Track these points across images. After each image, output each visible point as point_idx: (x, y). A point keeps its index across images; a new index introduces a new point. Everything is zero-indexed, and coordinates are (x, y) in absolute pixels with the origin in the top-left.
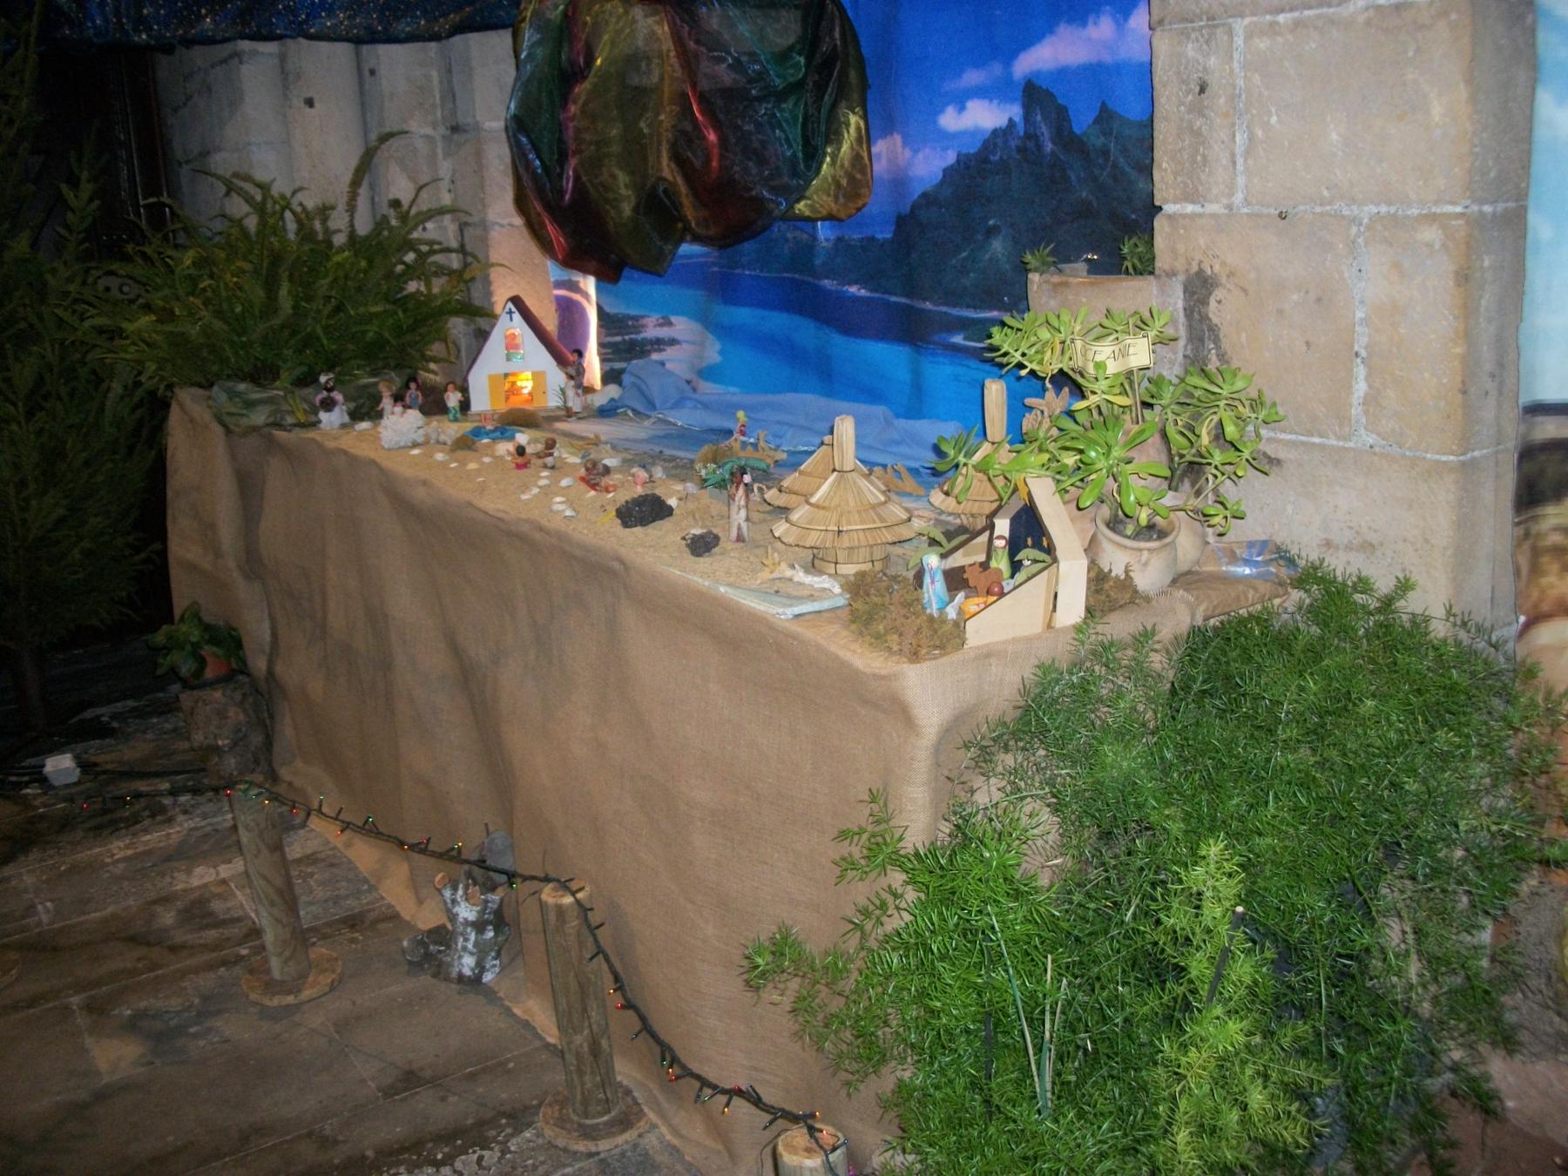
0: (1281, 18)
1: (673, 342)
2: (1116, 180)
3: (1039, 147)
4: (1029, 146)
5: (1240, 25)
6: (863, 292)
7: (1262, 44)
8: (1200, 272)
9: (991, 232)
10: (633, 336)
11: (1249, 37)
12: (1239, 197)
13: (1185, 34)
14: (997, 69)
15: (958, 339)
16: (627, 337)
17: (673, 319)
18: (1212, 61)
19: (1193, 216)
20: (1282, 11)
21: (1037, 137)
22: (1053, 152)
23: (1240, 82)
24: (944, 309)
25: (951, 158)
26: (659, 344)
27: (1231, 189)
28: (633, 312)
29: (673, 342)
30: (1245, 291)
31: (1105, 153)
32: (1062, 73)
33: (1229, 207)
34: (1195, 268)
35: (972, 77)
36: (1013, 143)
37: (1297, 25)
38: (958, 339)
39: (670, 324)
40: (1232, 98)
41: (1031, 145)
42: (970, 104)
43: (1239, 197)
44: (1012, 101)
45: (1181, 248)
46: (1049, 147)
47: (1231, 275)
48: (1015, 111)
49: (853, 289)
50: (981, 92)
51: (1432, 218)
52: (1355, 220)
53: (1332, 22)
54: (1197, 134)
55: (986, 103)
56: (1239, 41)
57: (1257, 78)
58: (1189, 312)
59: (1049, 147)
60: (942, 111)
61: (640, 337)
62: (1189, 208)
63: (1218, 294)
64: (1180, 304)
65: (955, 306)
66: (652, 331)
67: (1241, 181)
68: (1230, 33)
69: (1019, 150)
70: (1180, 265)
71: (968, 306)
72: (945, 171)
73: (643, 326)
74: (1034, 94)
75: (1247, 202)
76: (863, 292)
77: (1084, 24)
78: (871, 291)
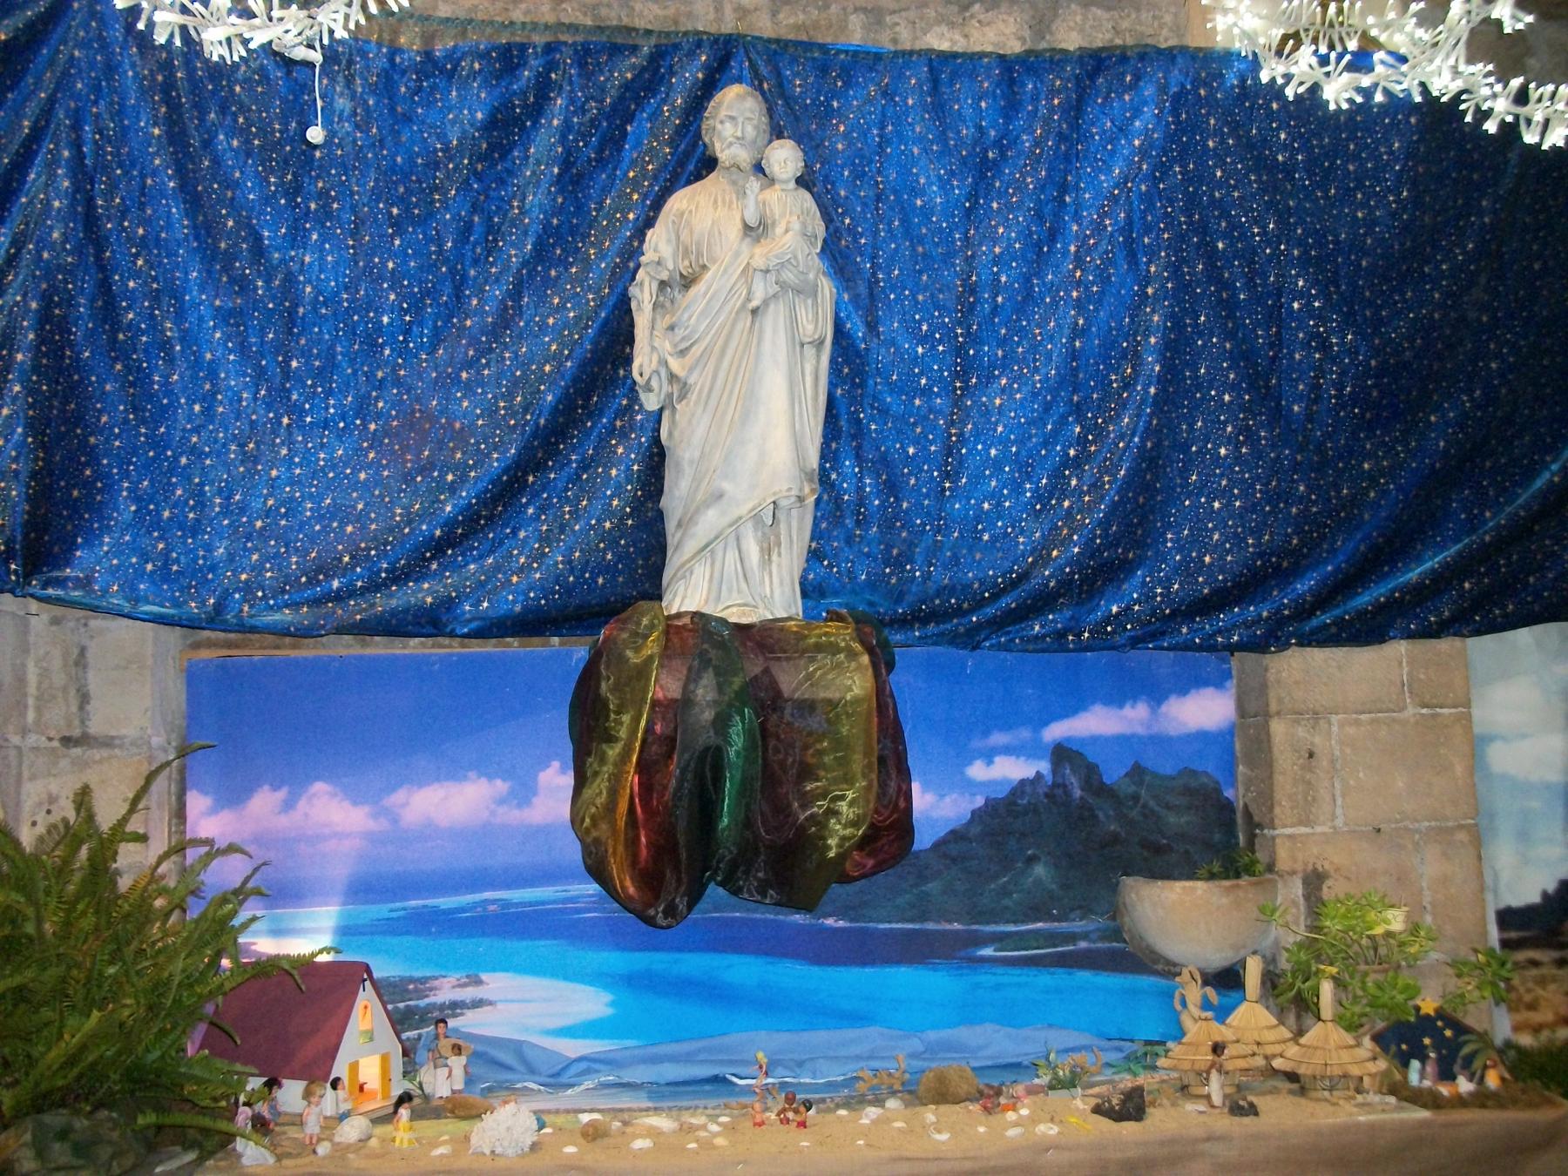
0: (1363, 717)
1: (478, 1004)
2: (1145, 816)
3: (1067, 793)
4: (1056, 793)
5: (1334, 718)
6: (841, 923)
7: (1351, 730)
8: (1315, 870)
9: (1031, 860)
10: (411, 1003)
11: (1342, 725)
12: (1339, 822)
13: (1297, 722)
14: (1025, 734)
15: (988, 952)
16: (401, 1005)
17: (484, 977)
18: (1317, 740)
19: (1308, 835)
20: (1363, 712)
21: (1065, 786)
22: (1082, 798)
23: (1337, 753)
24: (975, 927)
25: (979, 801)
26: (456, 1007)
27: (1334, 817)
28: (417, 974)
29: (478, 1004)
30: (1348, 879)
31: (1136, 798)
32: (1095, 740)
33: (1334, 827)
34: (1310, 867)
35: (998, 738)
36: (1041, 790)
37: (1373, 721)
38: (988, 952)
39: (479, 982)
40: (1332, 762)
41: (1059, 792)
42: (997, 759)
43: (1339, 822)
44: (1040, 758)
45: (1300, 856)
46: (1077, 793)
47: (1337, 870)
48: (1044, 766)
49: (830, 922)
50: (1008, 750)
51: (1461, 827)
52: (1417, 831)
53: (1394, 720)
54: (1309, 783)
55: (1013, 758)
56: (1335, 729)
57: (1348, 751)
58: (1307, 897)
59: (1077, 793)
60: (970, 763)
61: (422, 1003)
62: (1303, 830)
63: (1329, 883)
64: (1300, 892)
65: (988, 923)
66: (445, 993)
67: (1339, 811)
68: (1330, 723)
69: (1047, 795)
70: (1299, 867)
71: (1008, 922)
72: (973, 812)
73: (435, 989)
74: (1062, 754)
75: (1346, 824)
76: (841, 923)
77: (1121, 706)
78: (852, 920)
